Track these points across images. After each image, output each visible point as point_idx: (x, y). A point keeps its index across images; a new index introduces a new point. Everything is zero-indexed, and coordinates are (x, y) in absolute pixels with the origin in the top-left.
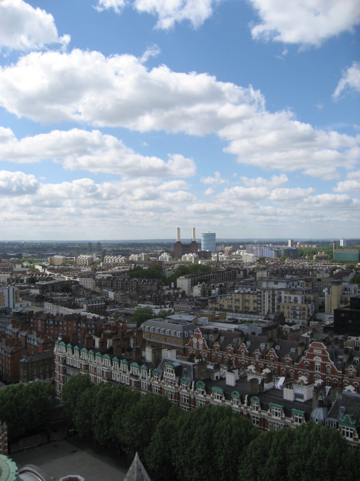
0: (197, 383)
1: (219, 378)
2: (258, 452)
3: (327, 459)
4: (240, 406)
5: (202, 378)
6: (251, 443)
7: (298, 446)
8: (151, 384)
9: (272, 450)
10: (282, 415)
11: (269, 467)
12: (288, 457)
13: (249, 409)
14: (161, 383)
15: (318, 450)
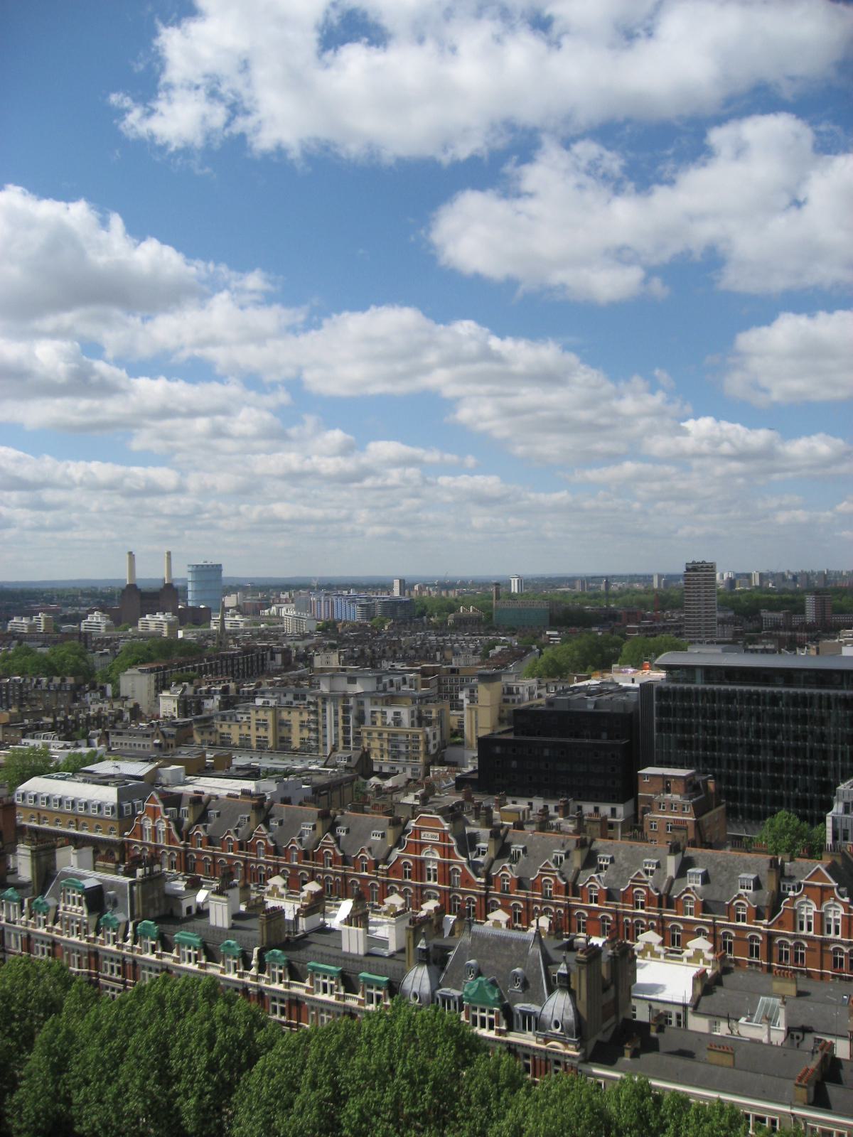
0: (138, 927)
1: (194, 911)
2: (273, 1081)
3: (431, 1084)
4: (241, 975)
5: (152, 913)
6: (260, 1063)
7: (365, 1060)
8: (29, 936)
9: (308, 1072)
10: (338, 990)
11: (300, 1114)
12: (343, 1087)
13: (263, 984)
15: (411, 1065)
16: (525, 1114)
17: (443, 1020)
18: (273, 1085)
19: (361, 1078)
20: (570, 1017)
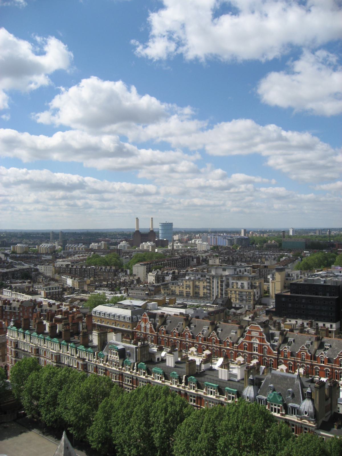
0: (139, 365)
1: (160, 360)
2: (190, 429)
3: (253, 434)
4: (178, 386)
5: (144, 360)
6: (185, 421)
7: (227, 423)
8: (97, 367)
9: (204, 426)
10: (216, 394)
11: (200, 442)
12: (218, 433)
13: (187, 390)
14: (106, 366)
16: (292, 449)
17: (259, 408)
18: (190, 430)
19: (225, 430)
20: (311, 410)
